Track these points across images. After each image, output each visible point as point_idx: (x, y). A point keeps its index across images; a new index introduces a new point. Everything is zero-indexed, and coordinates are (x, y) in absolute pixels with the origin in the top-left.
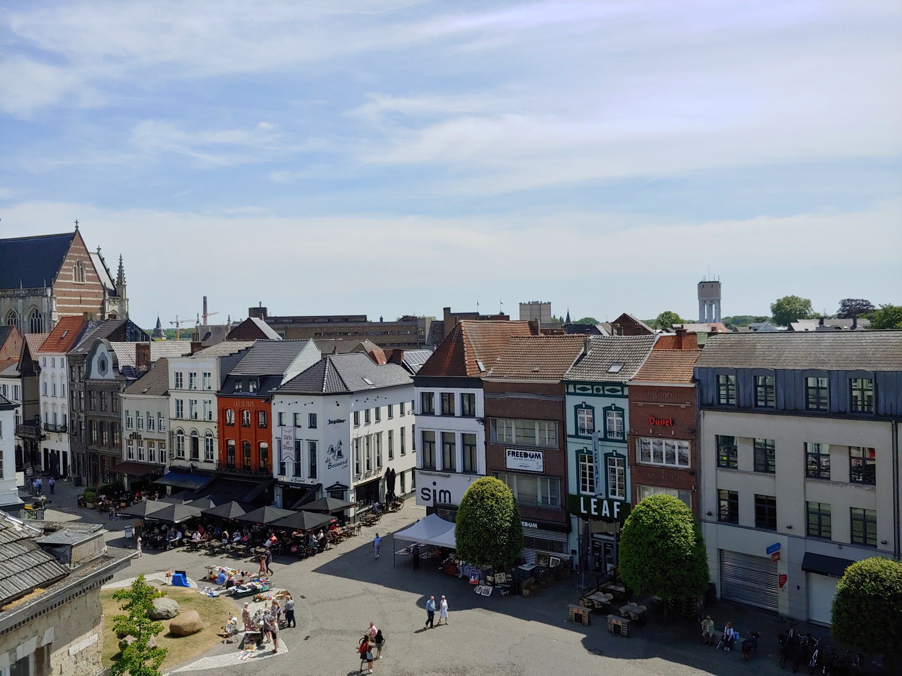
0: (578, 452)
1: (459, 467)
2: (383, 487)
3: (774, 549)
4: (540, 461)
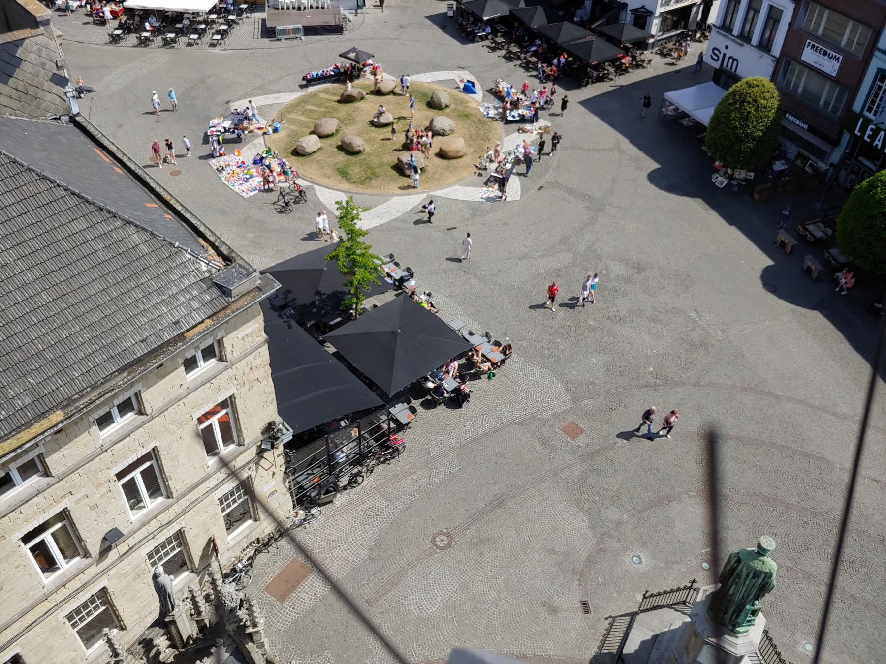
0: (879, 70)
1: (755, 39)
2: (697, 13)
4: (837, 65)
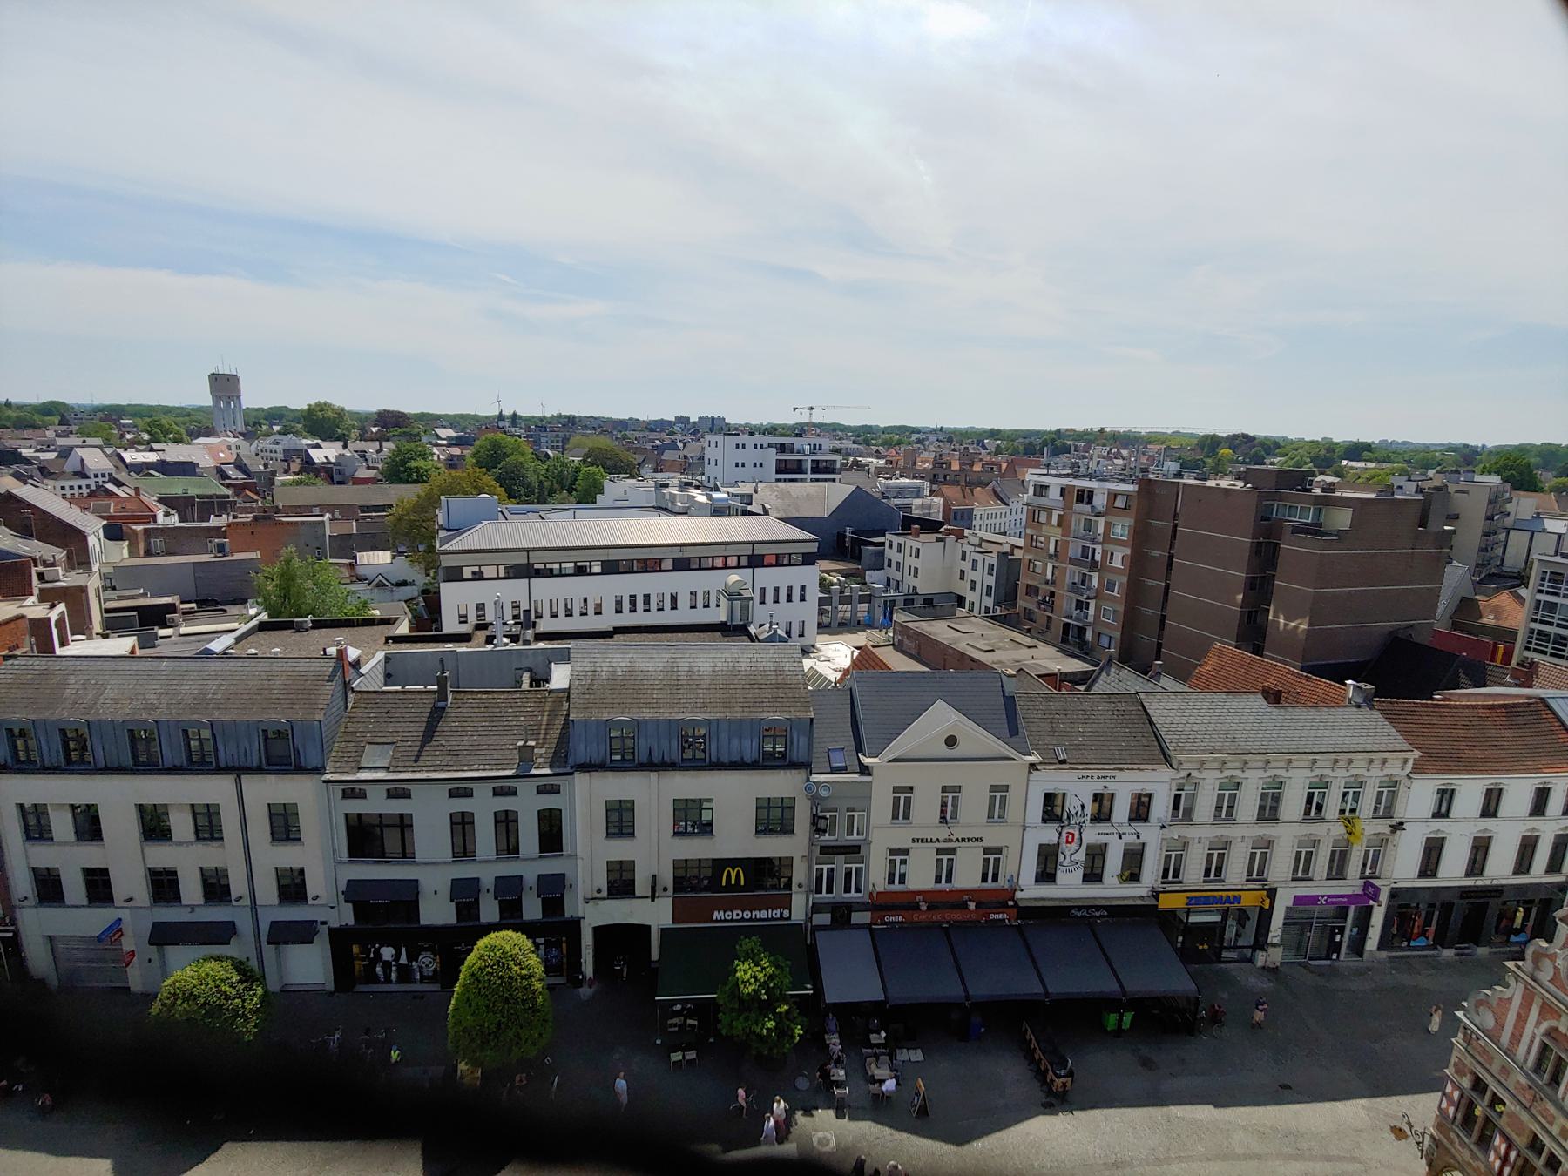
3: (116, 929)
